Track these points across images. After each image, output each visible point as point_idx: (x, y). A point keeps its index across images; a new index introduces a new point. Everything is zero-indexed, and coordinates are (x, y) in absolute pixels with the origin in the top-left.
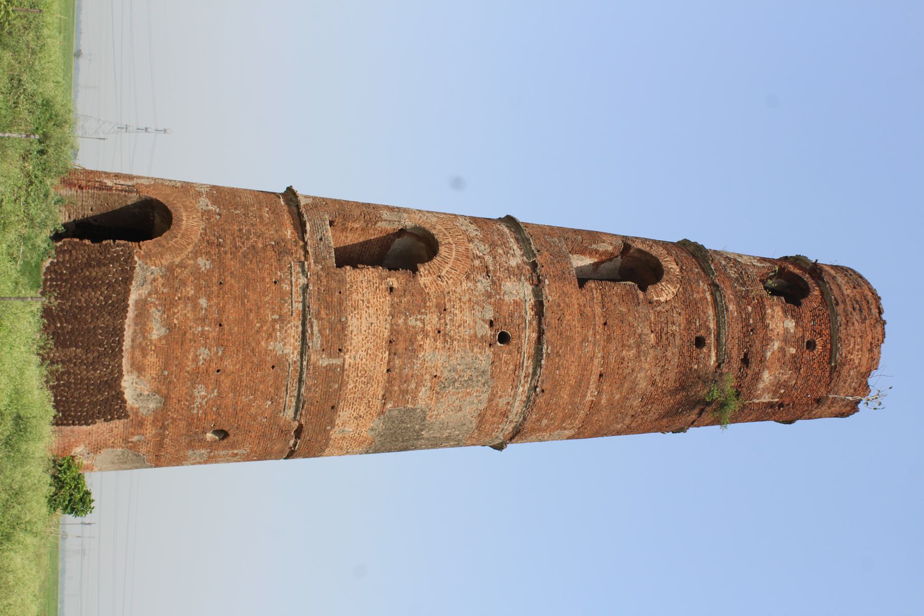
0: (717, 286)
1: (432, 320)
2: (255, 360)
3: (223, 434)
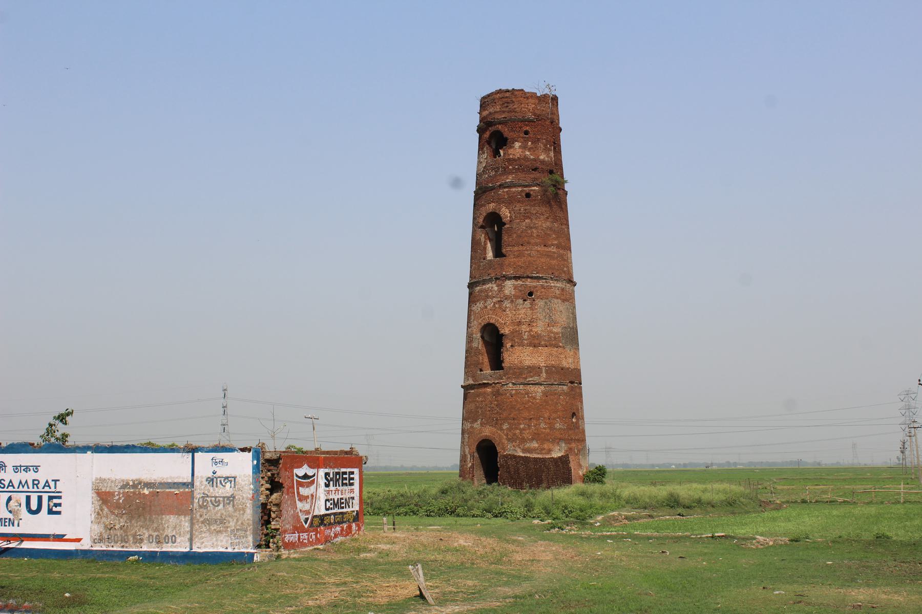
0: (500, 185)
1: (524, 328)
3: (574, 414)
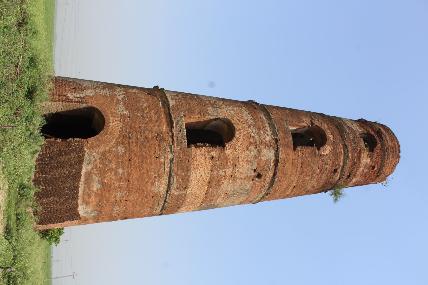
0: (346, 146)
1: (229, 171)
2: (145, 195)
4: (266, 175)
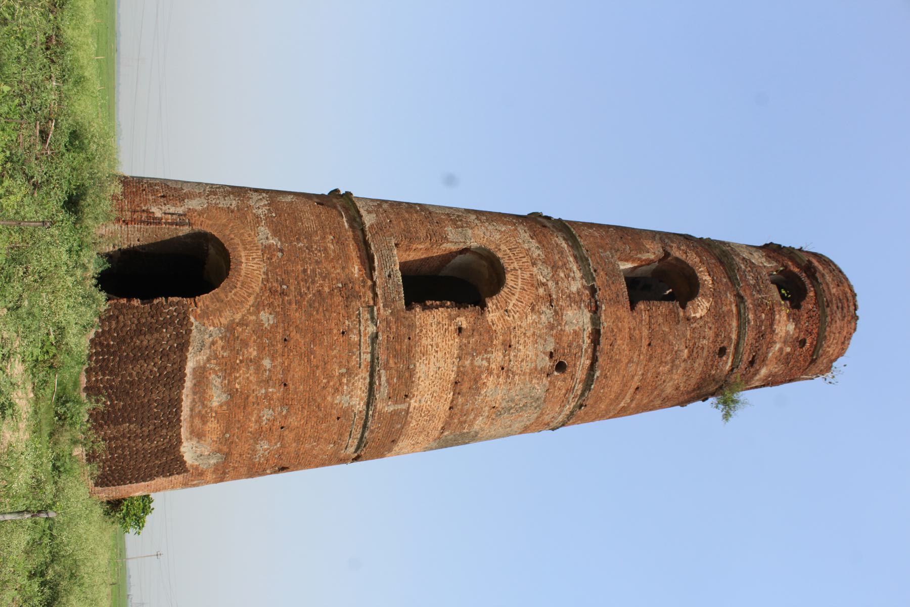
0: (741, 297)
1: (497, 357)
2: (321, 415)
4: (575, 365)
